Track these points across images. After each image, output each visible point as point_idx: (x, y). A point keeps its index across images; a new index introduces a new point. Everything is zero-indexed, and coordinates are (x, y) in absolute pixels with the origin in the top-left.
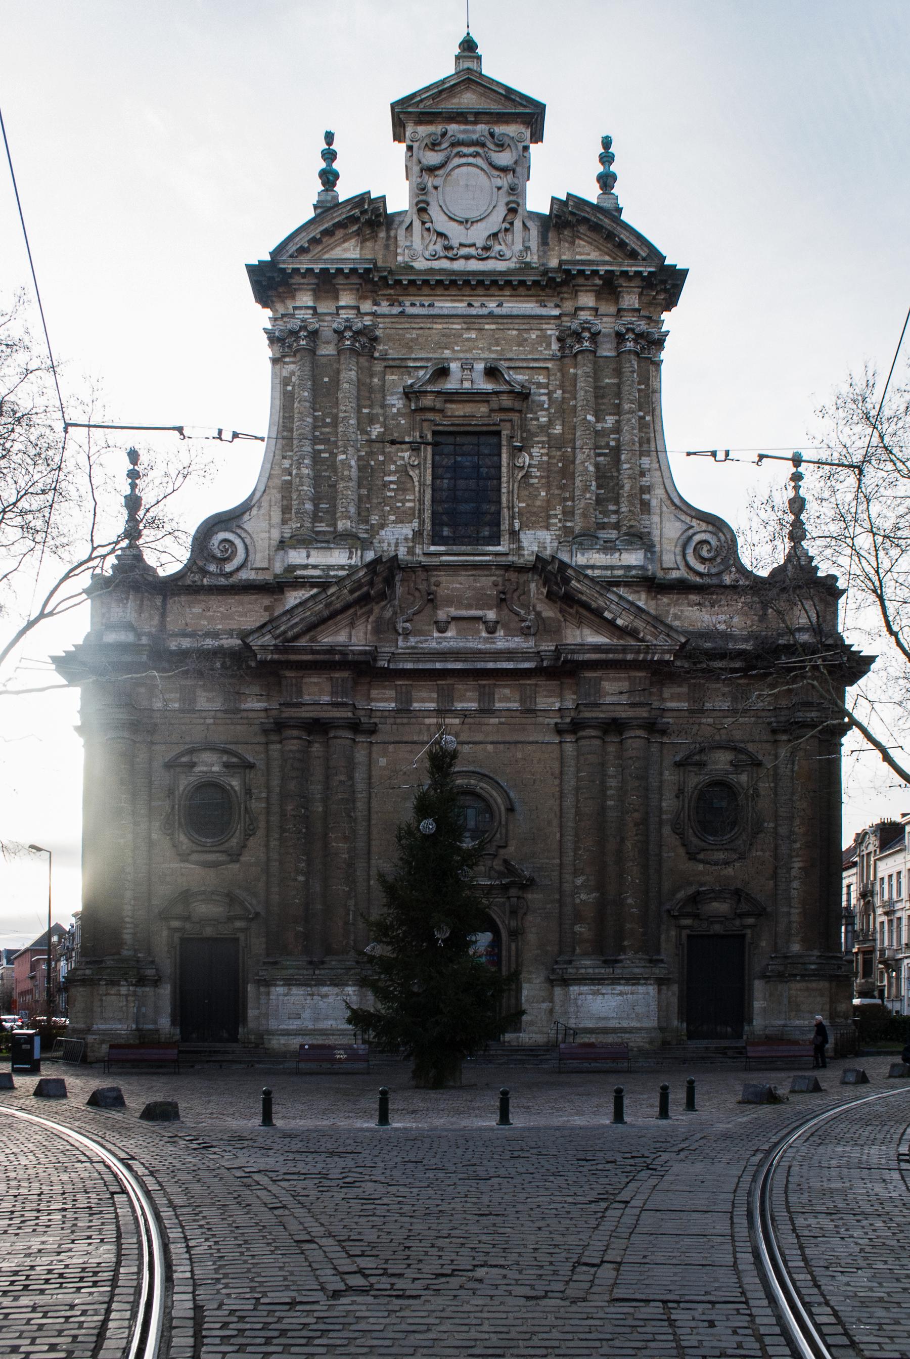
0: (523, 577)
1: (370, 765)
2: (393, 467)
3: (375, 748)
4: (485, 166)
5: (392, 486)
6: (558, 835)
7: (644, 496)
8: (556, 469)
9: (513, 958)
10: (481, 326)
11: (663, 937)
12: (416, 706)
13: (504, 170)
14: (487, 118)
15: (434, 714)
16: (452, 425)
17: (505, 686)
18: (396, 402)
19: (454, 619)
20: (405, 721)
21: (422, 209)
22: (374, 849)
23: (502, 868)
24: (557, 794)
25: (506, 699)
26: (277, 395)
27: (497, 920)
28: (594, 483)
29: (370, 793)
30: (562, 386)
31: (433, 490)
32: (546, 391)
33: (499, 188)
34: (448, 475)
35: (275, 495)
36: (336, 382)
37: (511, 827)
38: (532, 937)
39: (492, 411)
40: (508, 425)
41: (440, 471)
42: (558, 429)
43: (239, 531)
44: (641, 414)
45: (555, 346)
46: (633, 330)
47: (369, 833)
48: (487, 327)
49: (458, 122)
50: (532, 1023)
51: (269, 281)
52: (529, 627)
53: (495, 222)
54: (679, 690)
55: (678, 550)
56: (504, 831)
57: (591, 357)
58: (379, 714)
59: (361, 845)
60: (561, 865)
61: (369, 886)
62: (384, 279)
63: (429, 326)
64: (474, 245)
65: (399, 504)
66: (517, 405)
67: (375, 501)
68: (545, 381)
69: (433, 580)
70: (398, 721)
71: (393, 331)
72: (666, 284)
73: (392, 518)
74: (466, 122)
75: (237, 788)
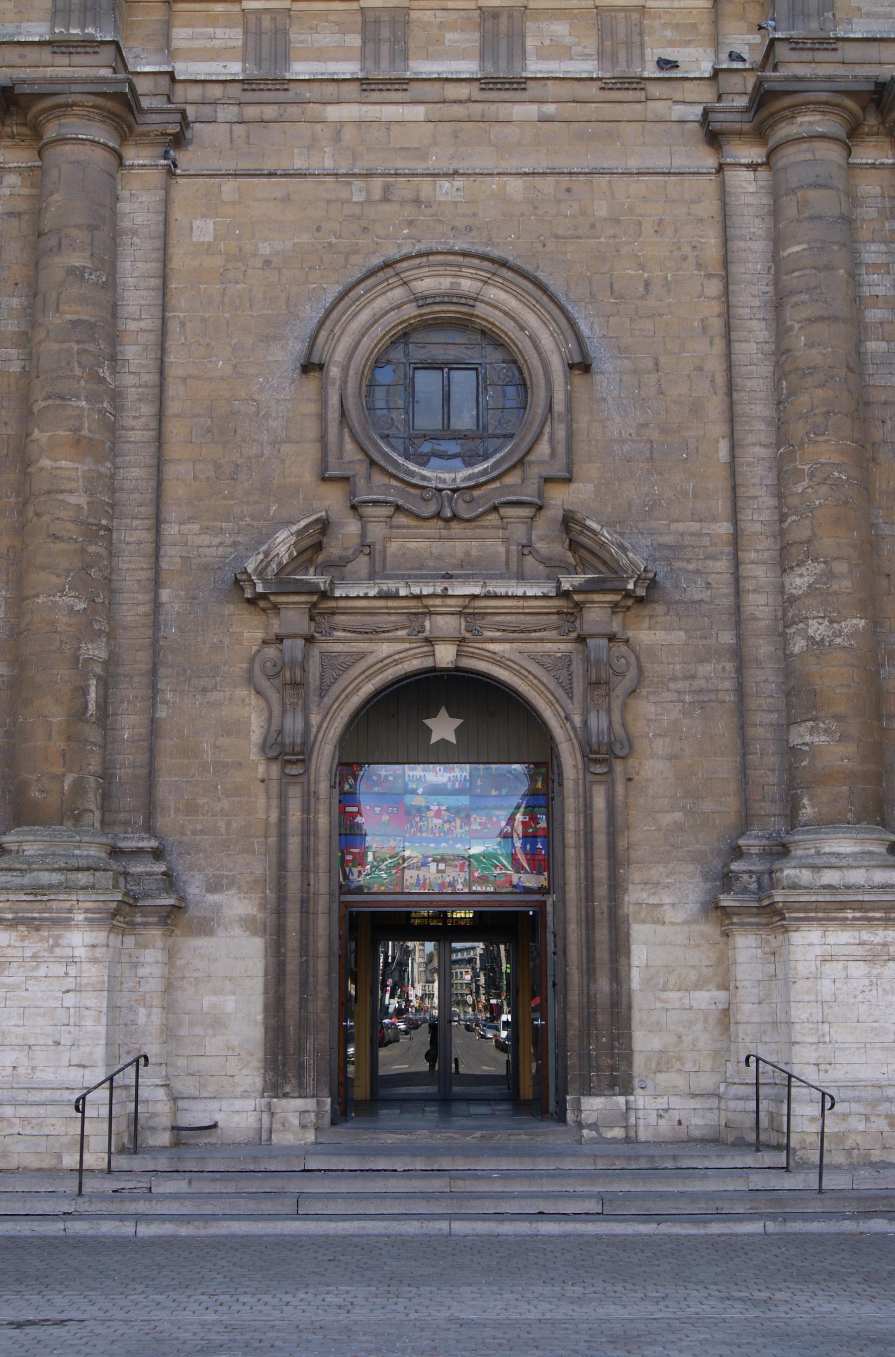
1: (165, 236)
3: (183, 188)
6: (723, 446)
9: (600, 839)
12: (300, 69)
20: (270, 112)
22: (175, 490)
24: (716, 325)
27: (548, 714)
29: (164, 321)
37: (583, 421)
38: (653, 767)
47: (160, 439)
50: (663, 1062)
56: (561, 433)
59: (135, 473)
60: (736, 539)
61: (157, 605)
70: (251, 112)
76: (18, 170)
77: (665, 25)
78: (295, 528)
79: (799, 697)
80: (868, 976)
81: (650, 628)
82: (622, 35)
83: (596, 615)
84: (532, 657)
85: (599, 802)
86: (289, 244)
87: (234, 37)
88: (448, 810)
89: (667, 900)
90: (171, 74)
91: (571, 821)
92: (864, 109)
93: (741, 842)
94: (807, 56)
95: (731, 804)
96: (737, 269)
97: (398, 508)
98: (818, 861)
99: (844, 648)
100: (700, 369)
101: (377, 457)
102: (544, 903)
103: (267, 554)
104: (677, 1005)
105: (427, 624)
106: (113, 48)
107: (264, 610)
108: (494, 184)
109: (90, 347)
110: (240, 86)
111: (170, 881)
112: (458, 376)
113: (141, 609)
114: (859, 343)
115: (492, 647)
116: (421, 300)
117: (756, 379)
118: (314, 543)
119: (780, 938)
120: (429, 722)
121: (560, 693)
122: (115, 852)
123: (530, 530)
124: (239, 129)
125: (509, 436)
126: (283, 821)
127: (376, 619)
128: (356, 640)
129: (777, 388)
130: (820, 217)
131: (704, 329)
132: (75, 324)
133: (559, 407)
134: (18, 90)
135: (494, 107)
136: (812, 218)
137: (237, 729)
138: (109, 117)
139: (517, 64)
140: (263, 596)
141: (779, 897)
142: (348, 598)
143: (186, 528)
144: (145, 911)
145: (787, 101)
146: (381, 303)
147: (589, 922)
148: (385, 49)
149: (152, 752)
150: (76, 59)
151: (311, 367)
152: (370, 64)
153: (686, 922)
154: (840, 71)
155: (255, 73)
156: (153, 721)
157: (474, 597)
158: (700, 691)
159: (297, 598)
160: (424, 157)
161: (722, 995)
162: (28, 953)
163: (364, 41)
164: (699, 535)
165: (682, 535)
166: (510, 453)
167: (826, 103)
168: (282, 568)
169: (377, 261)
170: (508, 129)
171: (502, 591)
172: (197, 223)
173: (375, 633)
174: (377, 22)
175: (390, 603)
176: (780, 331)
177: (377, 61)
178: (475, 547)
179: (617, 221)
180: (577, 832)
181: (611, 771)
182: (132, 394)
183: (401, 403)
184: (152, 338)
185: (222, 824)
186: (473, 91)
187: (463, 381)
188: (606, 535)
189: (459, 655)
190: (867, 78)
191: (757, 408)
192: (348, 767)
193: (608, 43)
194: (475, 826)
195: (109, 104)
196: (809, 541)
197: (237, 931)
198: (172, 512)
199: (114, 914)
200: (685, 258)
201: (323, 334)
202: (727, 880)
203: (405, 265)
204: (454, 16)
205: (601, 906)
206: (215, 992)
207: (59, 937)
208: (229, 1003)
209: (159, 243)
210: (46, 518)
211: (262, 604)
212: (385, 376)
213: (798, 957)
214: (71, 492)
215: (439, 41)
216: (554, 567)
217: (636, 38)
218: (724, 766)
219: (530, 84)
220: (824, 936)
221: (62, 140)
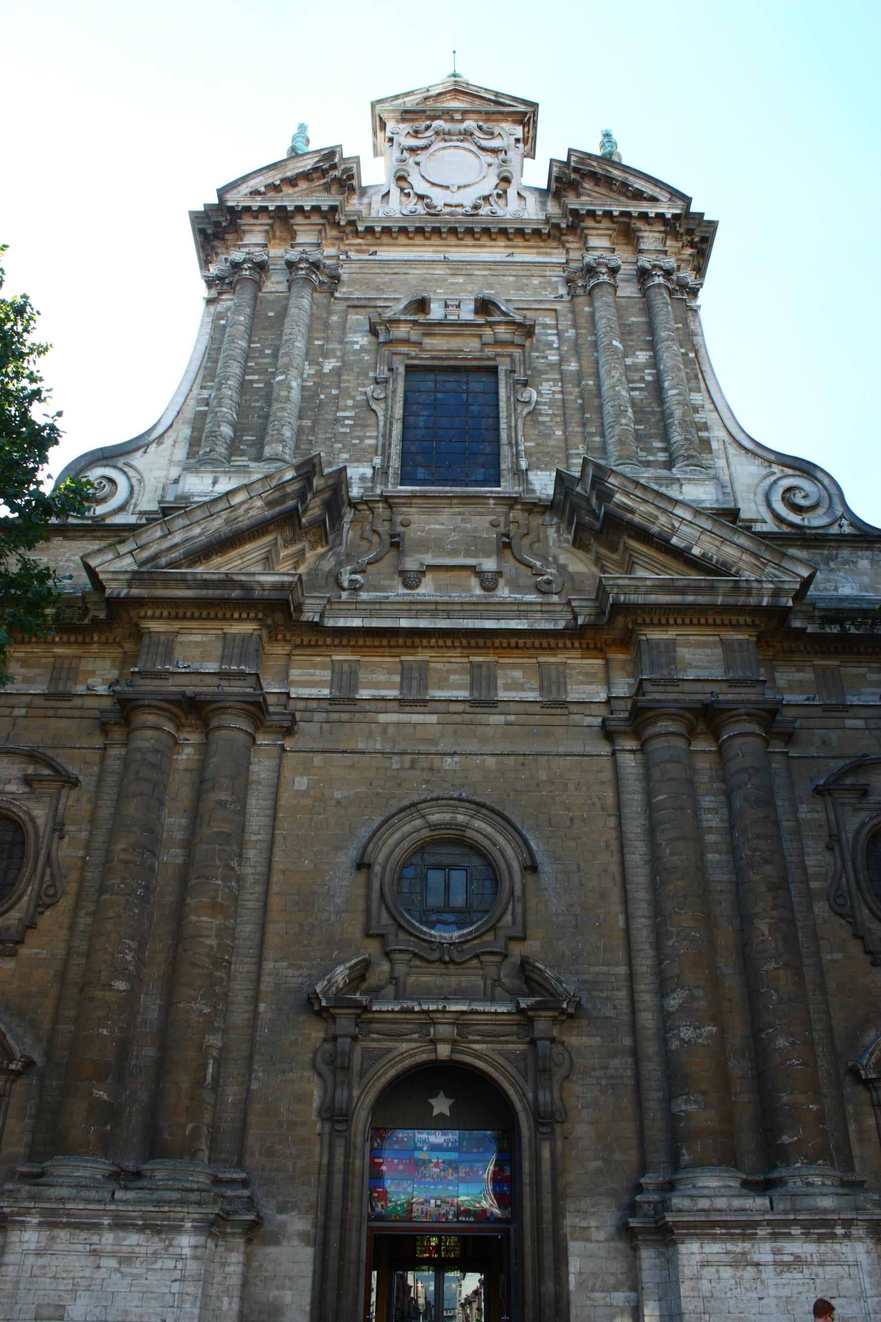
0: (536, 521)
1: (277, 785)
2: (350, 403)
3: (290, 760)
4: (474, 148)
5: (347, 422)
6: (621, 919)
7: (700, 434)
8: (575, 405)
9: (546, 1179)
10: (471, 272)
11: (852, 1128)
12: (364, 693)
13: (494, 151)
14: (475, 116)
15: (394, 705)
16: (432, 358)
17: (515, 666)
18: (361, 340)
19: (431, 568)
20: (345, 717)
21: (401, 178)
22: (273, 940)
23: (517, 983)
24: (614, 844)
25: (516, 682)
26: (208, 329)
27: (511, 1092)
28: (630, 410)
29: (273, 836)
30: (575, 326)
31: (404, 428)
32: (555, 332)
33: (490, 165)
34: (426, 413)
35: (186, 431)
36: (283, 314)
37: (532, 902)
38: (582, 1130)
39: (484, 344)
40: (507, 360)
41: (415, 408)
42: (573, 366)
43: (126, 469)
44: (683, 350)
45: (562, 291)
46: (661, 268)
47: (265, 907)
48: (477, 272)
49: (446, 121)
51: (215, 227)
52: (549, 582)
53: (489, 186)
54: (799, 676)
55: (760, 499)
56: (519, 910)
57: (611, 290)
58: (301, 705)
59: (247, 929)
60: (631, 977)
62: (352, 223)
63: (405, 271)
64: (462, 206)
65: (357, 441)
66: (517, 339)
67: (322, 436)
68: (553, 322)
69: (399, 518)
70: (334, 716)
71: (360, 276)
72: (695, 235)
73: (346, 456)
74: (452, 120)
75: (40, 822)
76: (193, 745)
77: (579, 673)
78: (348, 965)
79: (675, 1080)
80: (734, 1277)
81: (578, 1035)
82: (554, 677)
83: (541, 1026)
84: (500, 1053)
85: (546, 1153)
86: (352, 793)
87: (327, 675)
88: (444, 1162)
89: (593, 1223)
90: (288, 694)
91: (526, 1165)
92: (697, 719)
93: (642, 1180)
94: (661, 689)
95: (633, 1155)
96: (626, 811)
97: (416, 955)
98: (694, 1192)
99: (704, 1045)
100: (606, 871)
101: (402, 922)
102: (508, 1230)
103: (329, 981)
104: (602, 1303)
105: (432, 1030)
106: (254, 678)
107: (325, 1019)
108: (478, 760)
109: (227, 848)
110: (327, 702)
111: (251, 1203)
112: (455, 874)
113: (246, 1016)
114: (702, 855)
115: (475, 1046)
116: (432, 826)
117: (640, 876)
118: (360, 975)
119: (671, 1250)
120: (433, 1101)
121: (519, 1078)
122: (217, 1181)
123: (499, 971)
124: (325, 726)
125: (486, 911)
126: (331, 1163)
127: (398, 1026)
128: (385, 1040)
129: (653, 882)
130: (675, 779)
131: (607, 846)
132: (218, 834)
133: (518, 893)
134: (198, 698)
135: (478, 717)
136: (670, 780)
137: (304, 1098)
138: (249, 715)
139: (492, 693)
140: (326, 1009)
141: (669, 1218)
142: (381, 1012)
143: (279, 964)
144: (235, 1224)
145: (651, 714)
146: (407, 828)
147: (538, 1240)
148: (414, 683)
149: (245, 1112)
150: (233, 683)
151: (362, 865)
152: (405, 691)
153: (606, 1240)
154: (682, 697)
155: (337, 694)
156: (248, 1090)
157: (463, 1013)
158: (612, 1077)
159: (347, 1011)
160: (436, 744)
161: (633, 1295)
162: (150, 1250)
163: (402, 679)
164: (607, 974)
165: (597, 974)
166: (487, 922)
167: (674, 715)
168: (339, 990)
169: (406, 802)
170: (487, 729)
171: (481, 1009)
172: (297, 779)
173: (397, 1036)
174: (411, 668)
175: (408, 1016)
176: (653, 846)
177: (410, 690)
178: (464, 981)
179: (553, 783)
180: (531, 1174)
181: (553, 1132)
182: (250, 879)
183: (418, 890)
184: (265, 845)
185: (290, 1164)
186: (466, 707)
187: (458, 877)
188: (549, 973)
189: (453, 1051)
190: (698, 701)
191: (641, 894)
192: (379, 1132)
193: (545, 682)
194: (462, 1174)
195: (250, 708)
196: (678, 976)
197: (296, 1242)
198: (269, 954)
199: (213, 1223)
200: (594, 804)
201: (371, 846)
202: (633, 1209)
203: (423, 805)
204: (455, 666)
205: (547, 1227)
206: (278, 1288)
207: (173, 1239)
208: (288, 1297)
209: (273, 789)
210: (190, 953)
211: (325, 1015)
212: (409, 872)
213: (685, 1263)
214: (207, 937)
215: (447, 679)
216: (513, 995)
217: (562, 680)
218: (629, 1129)
219: (500, 704)
220: (701, 1247)
221: (221, 727)
